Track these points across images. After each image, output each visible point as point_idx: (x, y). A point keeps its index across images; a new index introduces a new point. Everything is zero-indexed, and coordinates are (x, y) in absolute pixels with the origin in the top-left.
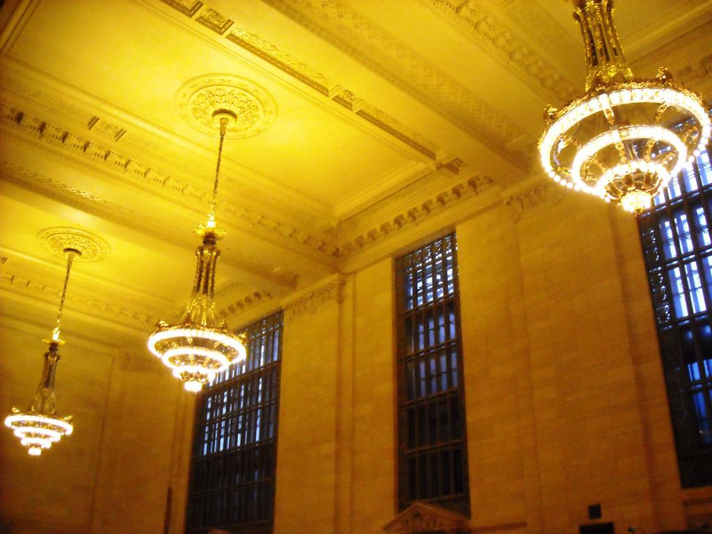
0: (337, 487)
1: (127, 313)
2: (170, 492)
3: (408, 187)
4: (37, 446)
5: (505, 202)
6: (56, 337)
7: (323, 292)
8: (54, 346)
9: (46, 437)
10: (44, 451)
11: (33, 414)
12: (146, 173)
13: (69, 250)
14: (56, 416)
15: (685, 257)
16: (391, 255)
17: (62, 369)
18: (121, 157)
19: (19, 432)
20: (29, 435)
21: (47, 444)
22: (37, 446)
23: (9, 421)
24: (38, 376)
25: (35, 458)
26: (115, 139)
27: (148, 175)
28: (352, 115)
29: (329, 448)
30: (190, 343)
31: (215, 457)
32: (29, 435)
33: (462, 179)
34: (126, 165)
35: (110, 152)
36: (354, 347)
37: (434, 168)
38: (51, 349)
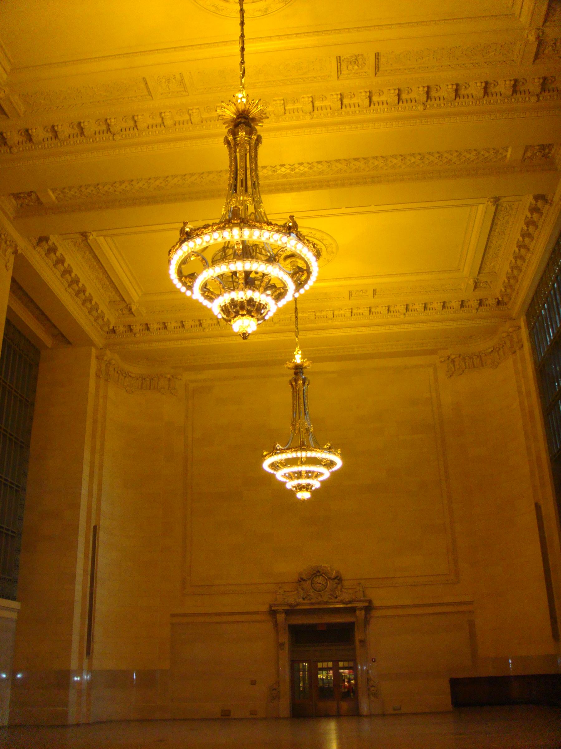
4: (301, 488)
6: (298, 359)
8: (298, 369)
10: (315, 493)
11: (282, 451)
21: (316, 484)
22: (307, 487)
23: (266, 465)
25: (303, 501)
38: (296, 374)
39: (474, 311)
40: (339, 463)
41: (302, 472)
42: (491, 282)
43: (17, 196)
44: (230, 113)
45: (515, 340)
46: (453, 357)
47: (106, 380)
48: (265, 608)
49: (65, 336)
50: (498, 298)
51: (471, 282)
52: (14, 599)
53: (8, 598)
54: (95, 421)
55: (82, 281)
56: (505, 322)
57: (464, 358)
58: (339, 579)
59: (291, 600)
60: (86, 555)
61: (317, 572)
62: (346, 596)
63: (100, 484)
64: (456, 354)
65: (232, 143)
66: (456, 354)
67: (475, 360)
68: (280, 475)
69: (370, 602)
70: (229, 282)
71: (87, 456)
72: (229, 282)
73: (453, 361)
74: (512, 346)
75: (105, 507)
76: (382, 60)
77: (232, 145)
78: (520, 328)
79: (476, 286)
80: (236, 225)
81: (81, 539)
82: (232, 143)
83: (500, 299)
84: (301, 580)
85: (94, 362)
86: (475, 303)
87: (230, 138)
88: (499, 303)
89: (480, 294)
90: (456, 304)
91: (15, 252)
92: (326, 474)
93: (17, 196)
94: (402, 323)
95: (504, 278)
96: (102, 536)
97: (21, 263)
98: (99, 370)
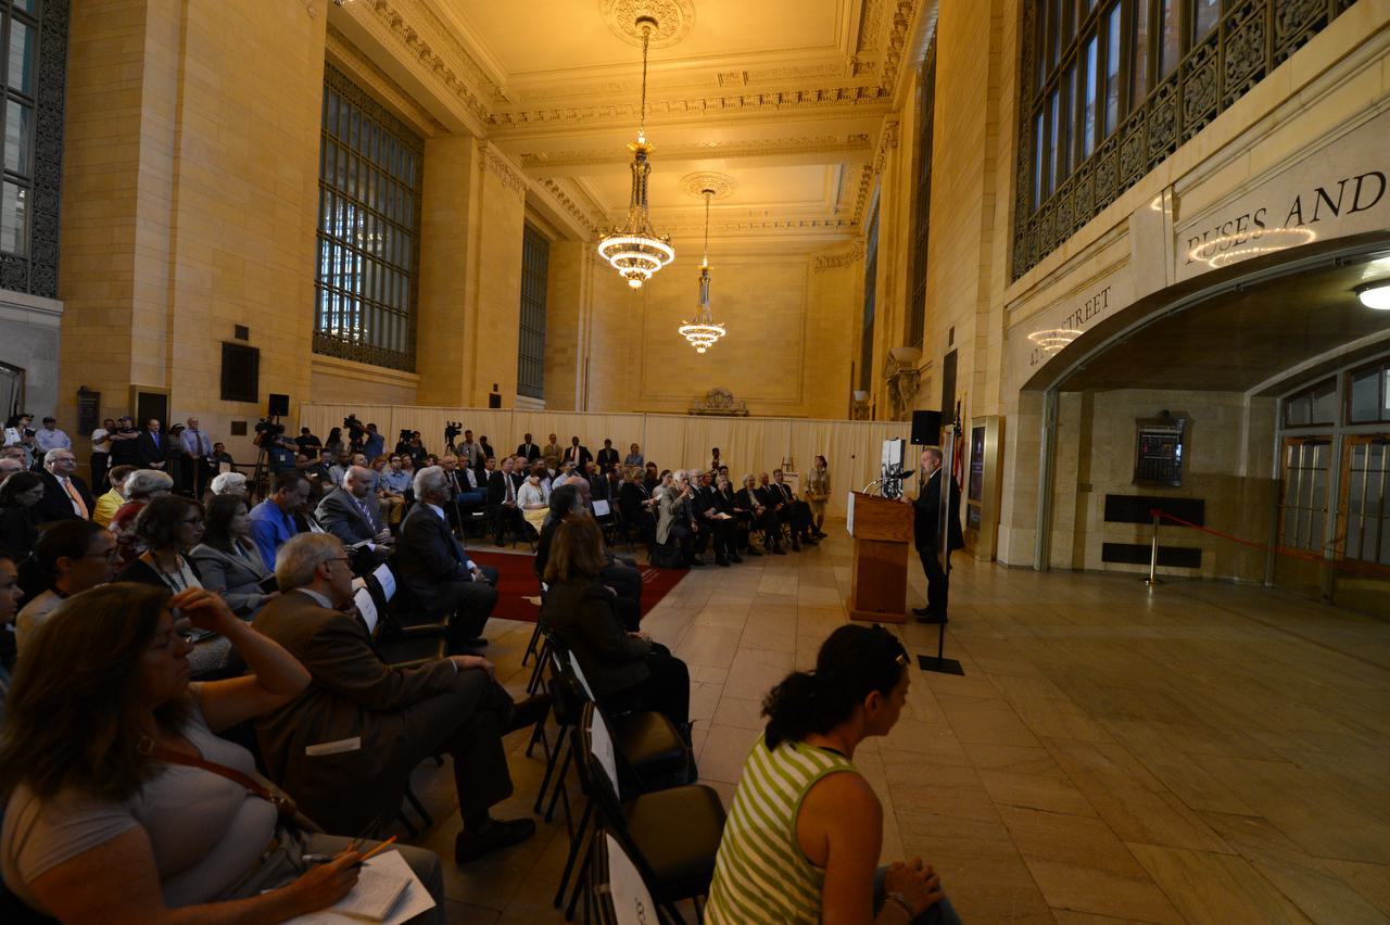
8: (705, 271)
9: (709, 339)
13: (707, 191)
14: (711, 324)
17: (715, 287)
19: (689, 337)
20: (696, 339)
21: (708, 344)
22: (702, 346)
24: (697, 298)
32: (696, 339)
40: (723, 333)
41: (702, 337)
43: (522, 155)
47: (593, 264)
48: (687, 411)
49: (563, 235)
51: (832, 209)
52: (542, 399)
53: (537, 398)
54: (586, 292)
55: (572, 200)
58: (730, 397)
59: (701, 408)
60: (582, 375)
61: (718, 393)
62: (733, 408)
63: (590, 333)
68: (689, 337)
69: (747, 412)
71: (581, 315)
75: (593, 346)
76: (749, 74)
79: (837, 211)
81: (579, 366)
84: (708, 397)
85: (584, 252)
91: (525, 189)
92: (715, 339)
93: (522, 155)
94: (784, 235)
95: (855, 203)
96: (592, 364)
97: (530, 194)
98: (588, 258)
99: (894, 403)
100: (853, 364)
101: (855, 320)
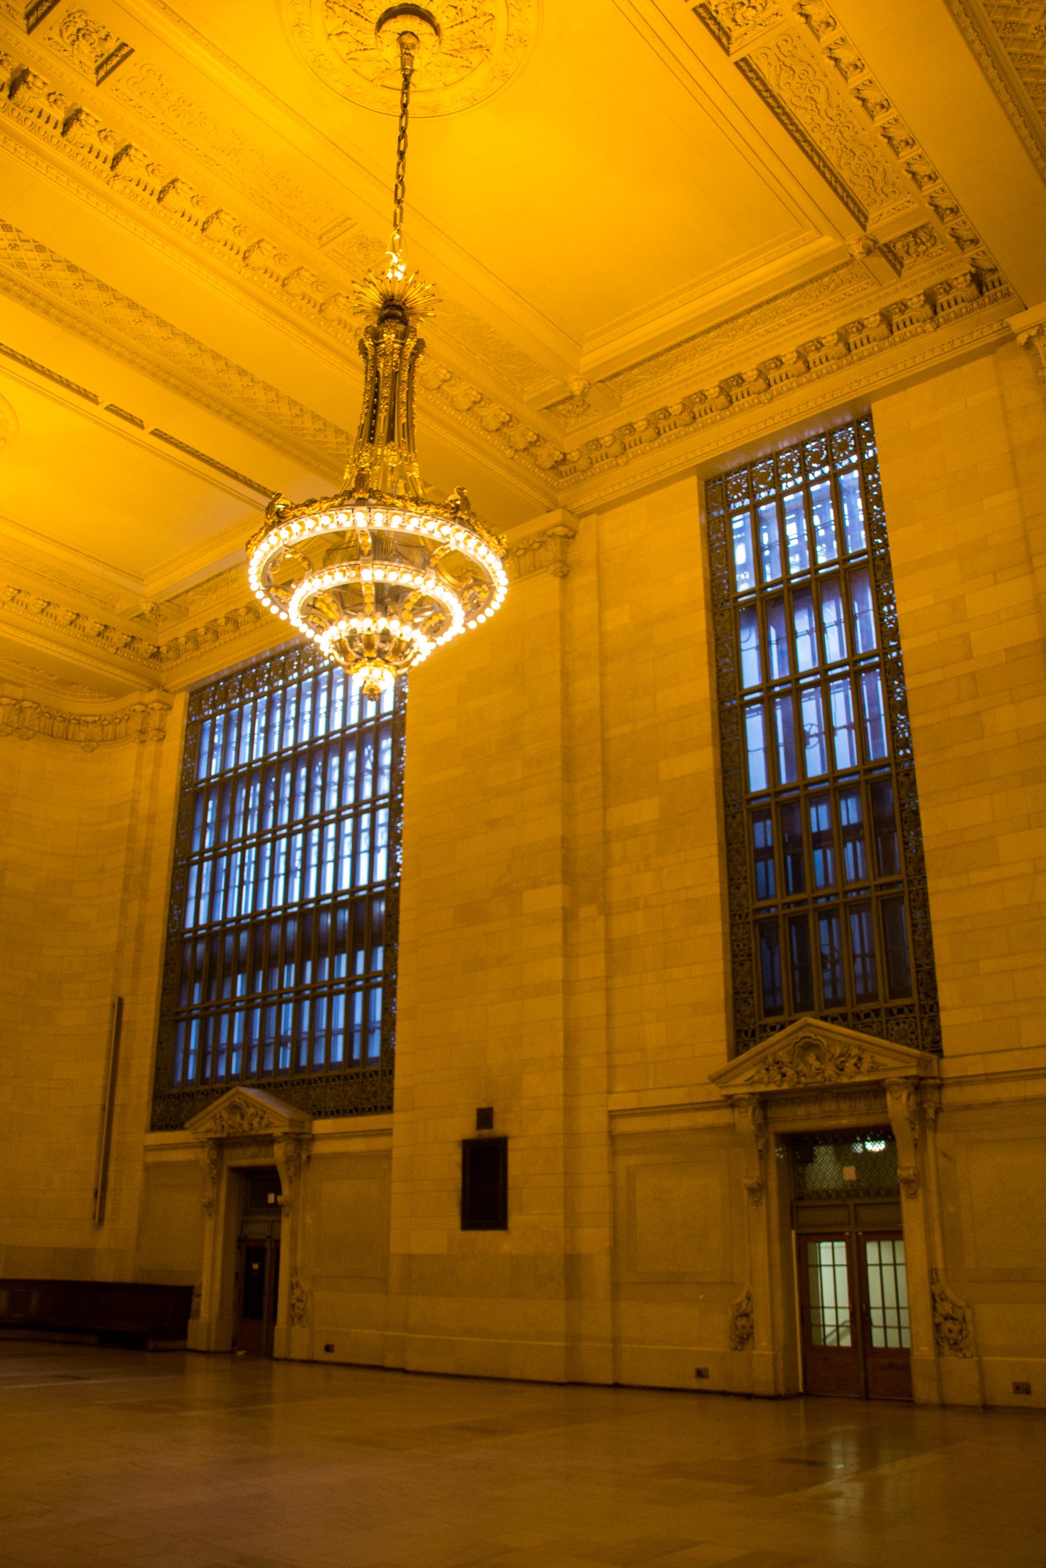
0: (569, 986)
1: (27, 600)
2: (119, 1005)
3: (765, 304)
5: (1022, 339)
7: (536, 545)
12: (163, 191)
15: (864, 659)
16: (699, 469)
18: (104, 134)
26: (94, 79)
27: (171, 195)
28: (725, 67)
29: (550, 898)
30: (367, 550)
31: (215, 933)
33: (910, 286)
34: (117, 160)
35: (79, 111)
36: (602, 675)
37: (857, 250)
39: (112, 650)
42: (166, 618)
44: (373, 297)
45: (154, 720)
46: (26, 704)
50: (159, 648)
56: (150, 690)
57: (42, 713)
64: (34, 703)
65: (371, 352)
66: (34, 703)
67: (56, 724)
70: (347, 598)
72: (347, 598)
73: (21, 710)
74: (142, 732)
77: (371, 356)
78: (170, 708)
80: (361, 502)
82: (371, 352)
83: (163, 649)
86: (119, 638)
87: (369, 343)
88: (156, 655)
89: (136, 628)
90: (92, 626)
99: (762, 1142)
100: (119, 1005)
101: (125, 888)
